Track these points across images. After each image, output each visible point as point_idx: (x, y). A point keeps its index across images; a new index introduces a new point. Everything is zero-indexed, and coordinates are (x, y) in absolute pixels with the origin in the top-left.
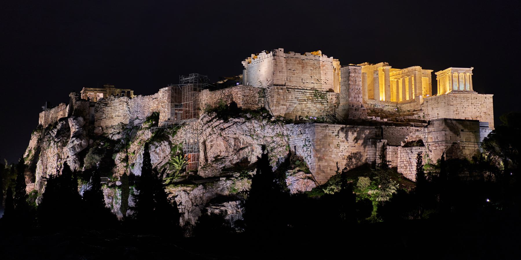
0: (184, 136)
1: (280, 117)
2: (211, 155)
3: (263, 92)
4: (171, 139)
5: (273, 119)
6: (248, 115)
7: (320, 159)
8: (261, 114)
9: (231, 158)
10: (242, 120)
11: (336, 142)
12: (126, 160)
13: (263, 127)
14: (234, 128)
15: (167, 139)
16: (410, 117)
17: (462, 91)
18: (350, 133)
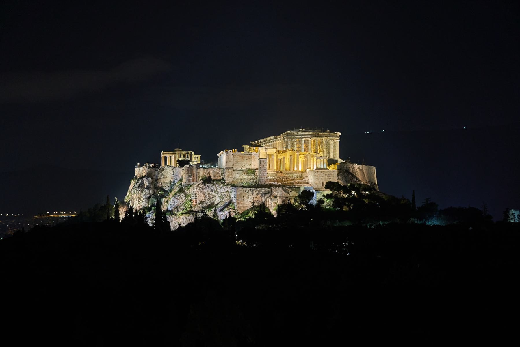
0: (191, 191)
1: (229, 183)
2: (198, 201)
3: (223, 171)
4: (186, 192)
5: (226, 184)
6: (215, 182)
7: (238, 203)
8: (221, 181)
9: (206, 202)
10: (211, 185)
11: (247, 196)
12: (167, 201)
13: (220, 188)
14: (207, 189)
15: (184, 192)
16: (300, 181)
17: (321, 169)
18: (254, 191)
